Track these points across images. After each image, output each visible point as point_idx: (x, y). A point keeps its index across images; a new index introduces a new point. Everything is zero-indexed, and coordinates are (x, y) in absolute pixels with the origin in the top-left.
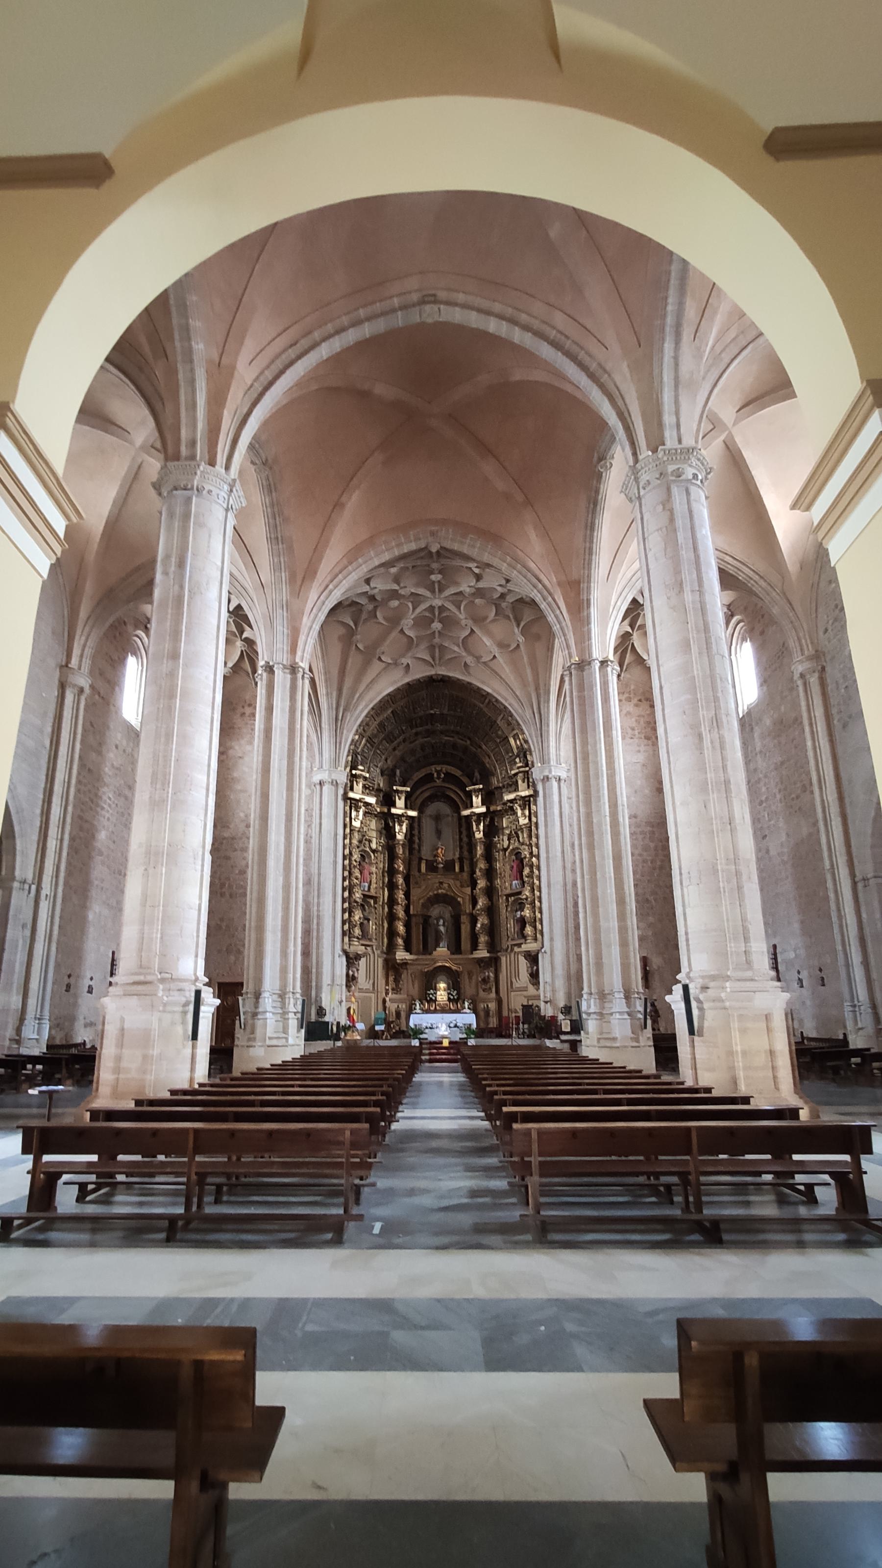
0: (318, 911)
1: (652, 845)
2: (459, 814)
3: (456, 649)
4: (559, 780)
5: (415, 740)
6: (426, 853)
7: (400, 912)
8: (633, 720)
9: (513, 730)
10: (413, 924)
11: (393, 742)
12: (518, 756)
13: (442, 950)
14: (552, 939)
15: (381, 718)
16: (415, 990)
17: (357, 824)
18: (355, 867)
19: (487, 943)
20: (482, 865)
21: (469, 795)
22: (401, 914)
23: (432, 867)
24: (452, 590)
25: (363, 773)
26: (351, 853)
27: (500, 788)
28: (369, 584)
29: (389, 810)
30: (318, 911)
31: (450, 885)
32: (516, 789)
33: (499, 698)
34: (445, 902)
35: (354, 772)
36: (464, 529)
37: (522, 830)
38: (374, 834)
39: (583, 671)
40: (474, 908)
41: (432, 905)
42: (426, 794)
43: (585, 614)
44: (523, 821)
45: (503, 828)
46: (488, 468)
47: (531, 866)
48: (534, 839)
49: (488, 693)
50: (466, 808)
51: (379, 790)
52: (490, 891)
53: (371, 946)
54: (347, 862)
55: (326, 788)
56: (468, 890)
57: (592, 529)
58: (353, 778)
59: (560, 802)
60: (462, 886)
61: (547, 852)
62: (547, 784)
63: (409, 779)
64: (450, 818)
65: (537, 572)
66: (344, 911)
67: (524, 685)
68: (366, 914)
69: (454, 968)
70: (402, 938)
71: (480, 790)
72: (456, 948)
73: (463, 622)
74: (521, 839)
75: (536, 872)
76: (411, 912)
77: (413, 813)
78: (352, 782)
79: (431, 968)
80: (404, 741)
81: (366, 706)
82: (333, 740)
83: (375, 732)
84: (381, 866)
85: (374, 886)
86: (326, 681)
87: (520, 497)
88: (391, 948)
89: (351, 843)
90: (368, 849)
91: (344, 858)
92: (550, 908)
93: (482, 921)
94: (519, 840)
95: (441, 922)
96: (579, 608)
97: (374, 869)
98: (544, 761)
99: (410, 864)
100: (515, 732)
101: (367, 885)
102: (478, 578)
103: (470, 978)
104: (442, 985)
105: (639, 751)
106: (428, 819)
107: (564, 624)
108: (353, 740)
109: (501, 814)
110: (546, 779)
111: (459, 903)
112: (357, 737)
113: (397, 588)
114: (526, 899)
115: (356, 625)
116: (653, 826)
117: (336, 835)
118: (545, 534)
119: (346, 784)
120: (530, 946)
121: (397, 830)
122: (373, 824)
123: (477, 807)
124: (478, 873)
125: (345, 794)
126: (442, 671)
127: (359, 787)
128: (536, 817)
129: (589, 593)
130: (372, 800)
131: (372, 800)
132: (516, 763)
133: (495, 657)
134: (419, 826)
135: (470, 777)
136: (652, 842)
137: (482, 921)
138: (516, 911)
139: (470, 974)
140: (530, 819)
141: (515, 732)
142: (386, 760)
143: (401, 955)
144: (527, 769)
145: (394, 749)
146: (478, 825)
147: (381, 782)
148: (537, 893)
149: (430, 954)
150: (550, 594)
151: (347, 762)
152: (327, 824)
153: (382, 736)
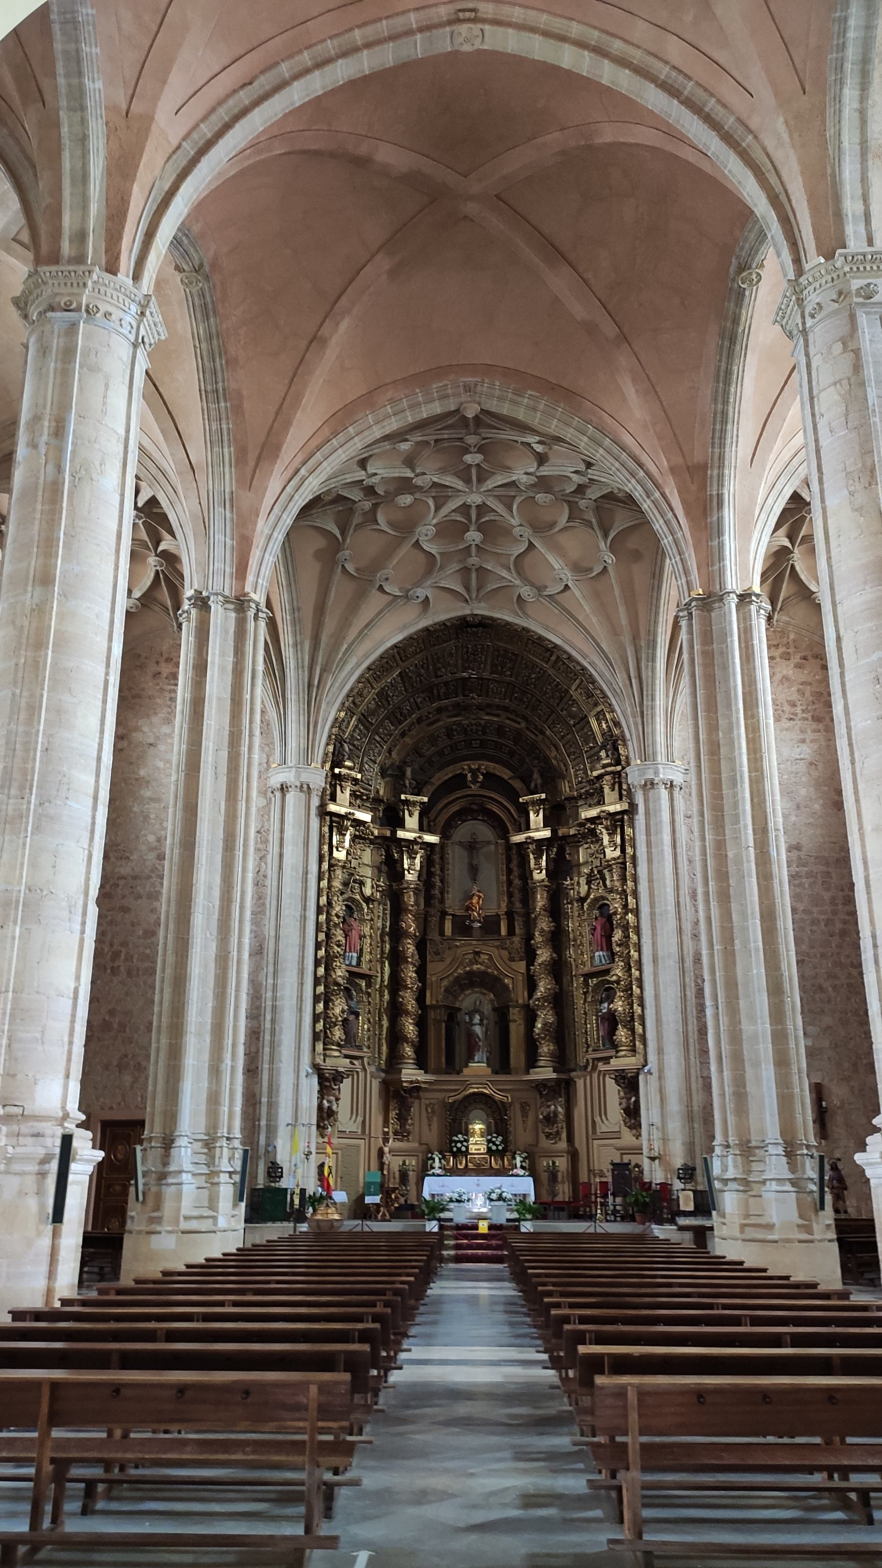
0: (274, 998)
1: (827, 896)
2: (507, 839)
3: (504, 573)
5: (437, 721)
6: (453, 903)
7: (409, 1000)
9: (596, 704)
12: (604, 747)
13: (478, 1067)
14: (660, 1051)
15: (382, 684)
17: (340, 855)
18: (336, 925)
19: (552, 1054)
20: (544, 924)
21: (524, 811)
23: (462, 927)
24: (500, 479)
25: (353, 774)
26: (329, 903)
27: (574, 798)
28: (365, 470)
29: (394, 833)
30: (274, 998)
31: (493, 957)
32: (601, 802)
33: (574, 653)
34: (482, 985)
35: (337, 771)
36: (519, 379)
37: (609, 867)
38: (368, 872)
39: (710, 611)
40: (530, 996)
42: (455, 808)
43: (715, 518)
44: (612, 853)
45: (579, 865)
46: (559, 282)
47: (626, 928)
48: (630, 883)
49: (556, 646)
50: (519, 831)
51: (377, 800)
53: (362, 1058)
54: (323, 918)
55: (290, 797)
56: (521, 966)
57: (727, 382)
58: (336, 780)
59: (673, 822)
60: (512, 959)
61: (652, 905)
63: (426, 783)
64: (492, 847)
65: (638, 451)
66: (316, 999)
67: (614, 631)
68: (353, 1004)
69: (498, 1097)
70: (413, 1045)
71: (542, 801)
72: (501, 1064)
73: (517, 531)
74: (608, 882)
75: (634, 937)
76: (428, 1002)
78: (333, 787)
79: (460, 1097)
80: (419, 720)
81: (358, 665)
82: (303, 719)
83: (372, 706)
84: (380, 925)
85: (367, 957)
86: (294, 622)
87: (610, 330)
89: (330, 887)
90: (358, 897)
92: (657, 997)
93: (545, 1017)
94: (605, 885)
95: (477, 1018)
96: (705, 510)
97: (367, 930)
98: (647, 755)
99: (425, 920)
100: (599, 709)
101: (355, 955)
102: (542, 459)
103: (525, 1114)
105: (803, 741)
106: (457, 848)
107: (679, 535)
108: (336, 719)
109: (575, 841)
110: (650, 785)
111: (506, 987)
112: (342, 714)
113: (410, 474)
114: (618, 982)
115: (343, 533)
116: (827, 864)
117: (306, 873)
118: (651, 390)
119: (324, 790)
120: (624, 1062)
121: (406, 866)
122: (367, 855)
123: (537, 830)
124: (538, 938)
125: (322, 806)
126: (482, 609)
127: (344, 796)
128: (634, 847)
129: (720, 485)
130: (365, 816)
131: (365, 816)
132: (600, 759)
133: (567, 587)
134: (442, 858)
135: (526, 780)
136: (828, 889)
137: (545, 1017)
138: (601, 1002)
140: (623, 851)
141: (599, 709)
142: (390, 752)
143: (410, 1074)
144: (619, 768)
145: (403, 735)
146: (538, 858)
147: (381, 787)
148: (635, 973)
149: (459, 1072)
150: (658, 486)
151: (326, 754)
152: (292, 855)
153: (383, 713)
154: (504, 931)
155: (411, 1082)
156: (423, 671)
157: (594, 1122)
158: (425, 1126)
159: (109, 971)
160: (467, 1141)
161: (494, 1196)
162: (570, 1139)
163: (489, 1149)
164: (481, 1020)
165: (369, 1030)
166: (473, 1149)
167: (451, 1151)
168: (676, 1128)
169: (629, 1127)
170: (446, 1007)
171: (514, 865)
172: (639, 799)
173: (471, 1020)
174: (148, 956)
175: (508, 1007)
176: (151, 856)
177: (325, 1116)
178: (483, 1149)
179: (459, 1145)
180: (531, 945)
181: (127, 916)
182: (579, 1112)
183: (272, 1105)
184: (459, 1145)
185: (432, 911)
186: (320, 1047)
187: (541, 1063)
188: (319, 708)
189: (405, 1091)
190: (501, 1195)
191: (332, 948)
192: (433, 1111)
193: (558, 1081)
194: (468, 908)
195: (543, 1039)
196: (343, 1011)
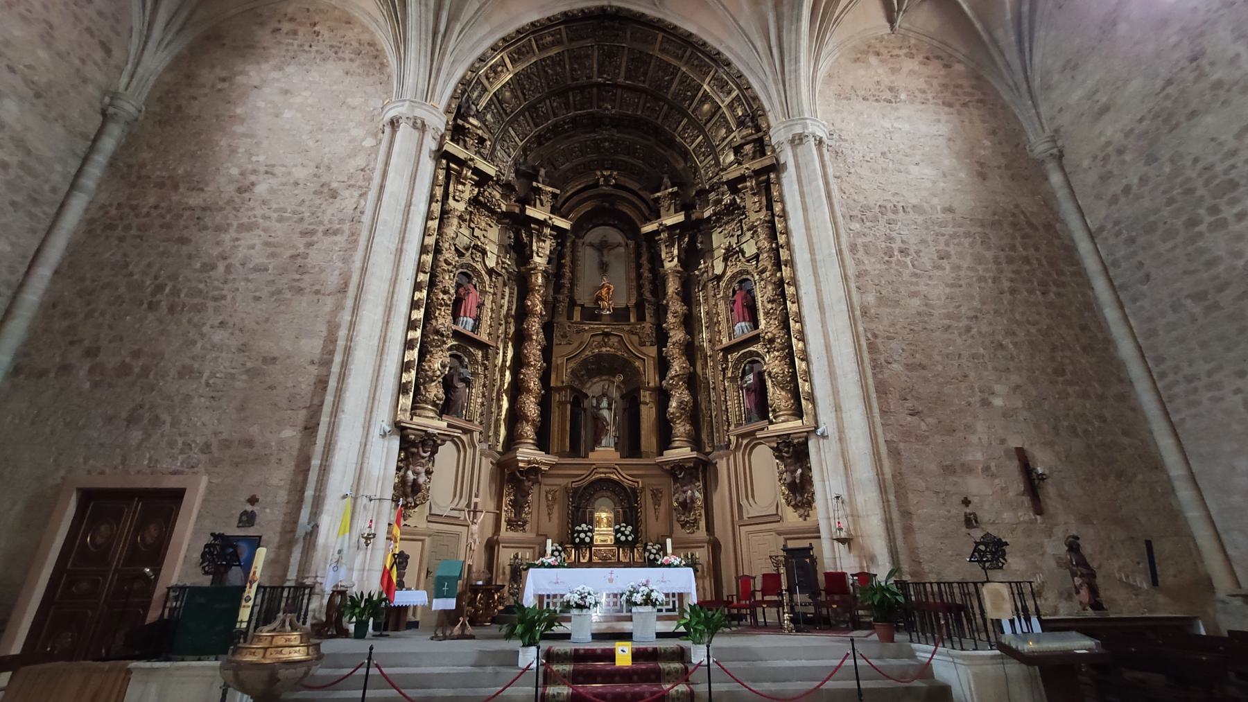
0: (350, 338)
1: (989, 255)
4: (820, 142)
6: (584, 296)
8: (922, 80)
11: (536, 125)
13: (606, 453)
14: (838, 408)
16: (553, 523)
19: (688, 435)
20: (676, 308)
22: (534, 384)
23: (592, 314)
35: (460, 122)
40: (663, 376)
41: (590, 377)
52: (690, 350)
56: (652, 351)
60: (642, 344)
61: (812, 252)
62: (800, 149)
64: (622, 250)
69: (627, 483)
70: (533, 424)
72: (630, 445)
79: (585, 482)
81: (491, 32)
88: (513, 440)
90: (479, 267)
91: (424, 250)
95: (604, 404)
101: (471, 321)
103: (657, 503)
104: (604, 515)
105: (939, 121)
106: (589, 250)
110: (797, 141)
111: (637, 370)
116: (983, 226)
117: (409, 205)
136: (989, 249)
143: (527, 453)
149: (586, 456)
155: (529, 462)
157: (740, 506)
158: (544, 513)
159: (145, 306)
160: (591, 531)
162: (710, 528)
163: (617, 540)
164: (610, 405)
165: (482, 404)
166: (598, 539)
167: (573, 542)
168: (869, 502)
169: (796, 507)
170: (572, 388)
171: (644, 260)
172: (787, 157)
174: (201, 292)
175: (638, 390)
176: (230, 190)
177: (408, 493)
178: (610, 539)
179: (582, 535)
180: (663, 329)
181: (184, 248)
183: (324, 470)
184: (582, 535)
185: (561, 297)
186: (406, 401)
187: (677, 444)
188: (444, 55)
189: (521, 472)
191: (435, 294)
192: (554, 499)
194: (599, 298)
195: (679, 418)
196: (443, 366)
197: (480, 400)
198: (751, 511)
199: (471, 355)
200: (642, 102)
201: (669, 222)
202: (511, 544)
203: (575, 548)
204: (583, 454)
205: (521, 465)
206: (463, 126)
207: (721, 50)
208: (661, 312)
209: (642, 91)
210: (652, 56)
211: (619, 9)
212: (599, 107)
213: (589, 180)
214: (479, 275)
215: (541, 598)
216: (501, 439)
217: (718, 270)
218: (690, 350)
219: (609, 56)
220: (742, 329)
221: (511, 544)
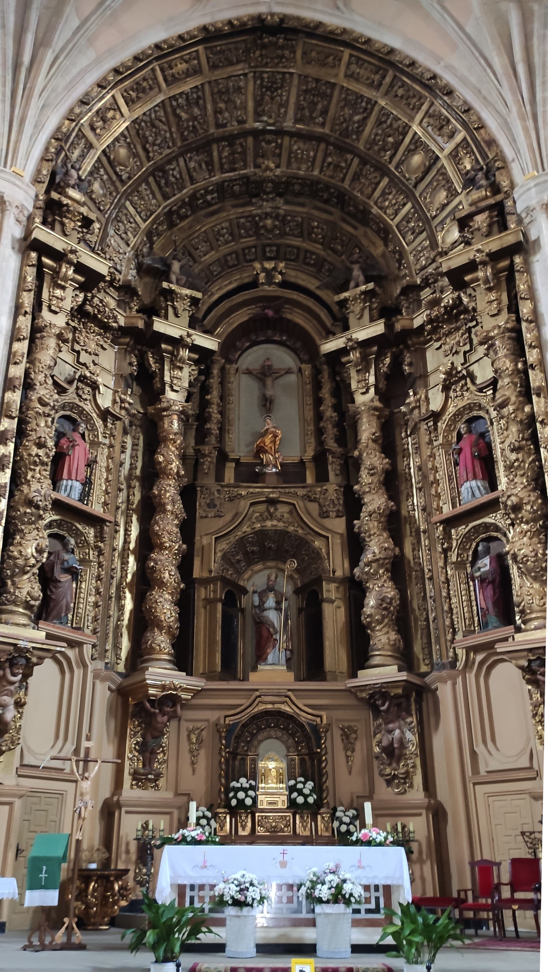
6: (239, 447)
7: (168, 570)
10: (199, 604)
11: (166, 197)
13: (273, 674)
19: (394, 647)
20: (373, 460)
23: (250, 473)
29: (149, 324)
40: (354, 561)
41: (250, 563)
52: (395, 523)
53: (78, 645)
56: (339, 525)
60: (324, 515)
64: (293, 378)
69: (304, 718)
70: (169, 632)
72: (310, 663)
76: (196, 574)
77: (209, 343)
79: (244, 717)
81: (97, 61)
88: (139, 656)
90: (88, 407)
95: (271, 602)
101: (78, 486)
106: (245, 380)
111: (316, 556)
124: (365, 477)
137: (380, 592)
139: (348, 735)
143: (161, 674)
144: (499, 197)
149: (245, 678)
154: (310, 480)
155: (163, 687)
156: (196, 111)
157: (474, 754)
158: (186, 763)
160: (253, 788)
161: (324, 892)
162: (429, 786)
163: (292, 803)
165: (96, 605)
166: (263, 801)
167: (227, 805)
170: (224, 580)
171: (326, 393)
173: (262, 602)
175: (318, 581)
178: (282, 802)
179: (241, 795)
180: (354, 493)
182: (444, 741)
184: (241, 795)
185: (206, 449)
187: (376, 660)
188: (29, 98)
189: (152, 702)
190: (339, 888)
191: (26, 448)
192: (200, 741)
193: (407, 685)
194: (261, 450)
195: (379, 622)
196: (40, 551)
197: (92, 599)
198: (490, 762)
199: (78, 534)
200: (320, 155)
201: (362, 335)
202: (138, 808)
203: (231, 814)
204: (240, 675)
205: (151, 691)
206: (60, 204)
207: (438, 70)
208: (351, 467)
209: (321, 139)
210: (334, 84)
211: (284, 18)
212: (257, 166)
213: (246, 277)
214: (89, 420)
215: (181, 889)
216: (124, 654)
217: (436, 404)
218: (395, 523)
219: (270, 88)
220: (472, 491)
221: (138, 808)
